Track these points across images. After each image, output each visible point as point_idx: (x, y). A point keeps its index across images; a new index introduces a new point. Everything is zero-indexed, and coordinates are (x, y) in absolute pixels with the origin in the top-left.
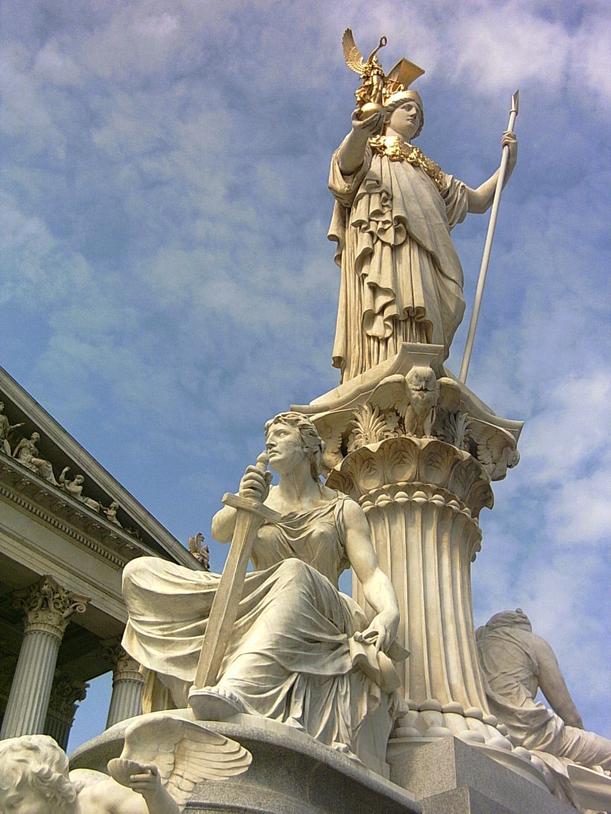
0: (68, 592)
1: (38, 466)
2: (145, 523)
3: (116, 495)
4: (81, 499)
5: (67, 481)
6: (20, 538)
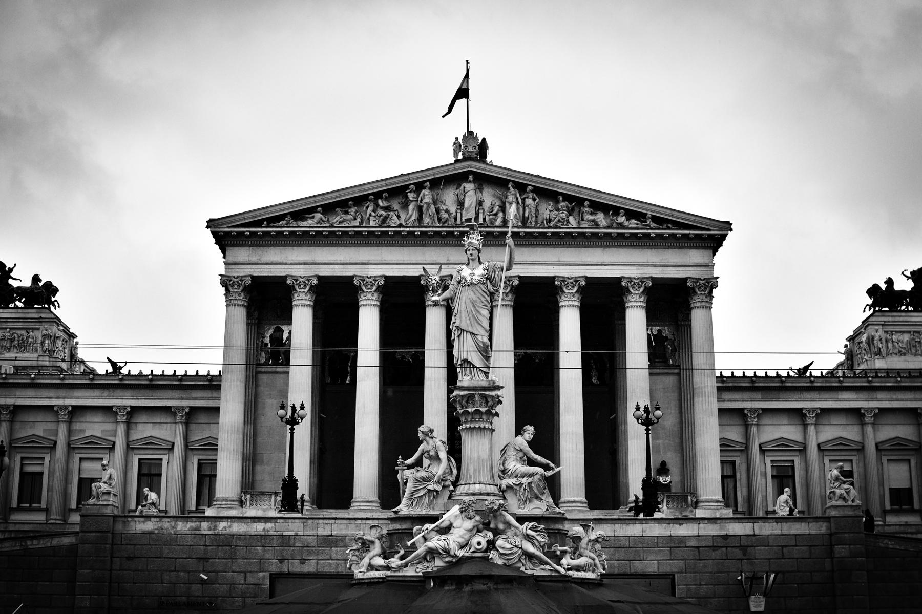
0: (638, 278)
1: (593, 221)
2: (672, 216)
3: (646, 210)
4: (626, 223)
5: (615, 217)
6: (600, 263)
